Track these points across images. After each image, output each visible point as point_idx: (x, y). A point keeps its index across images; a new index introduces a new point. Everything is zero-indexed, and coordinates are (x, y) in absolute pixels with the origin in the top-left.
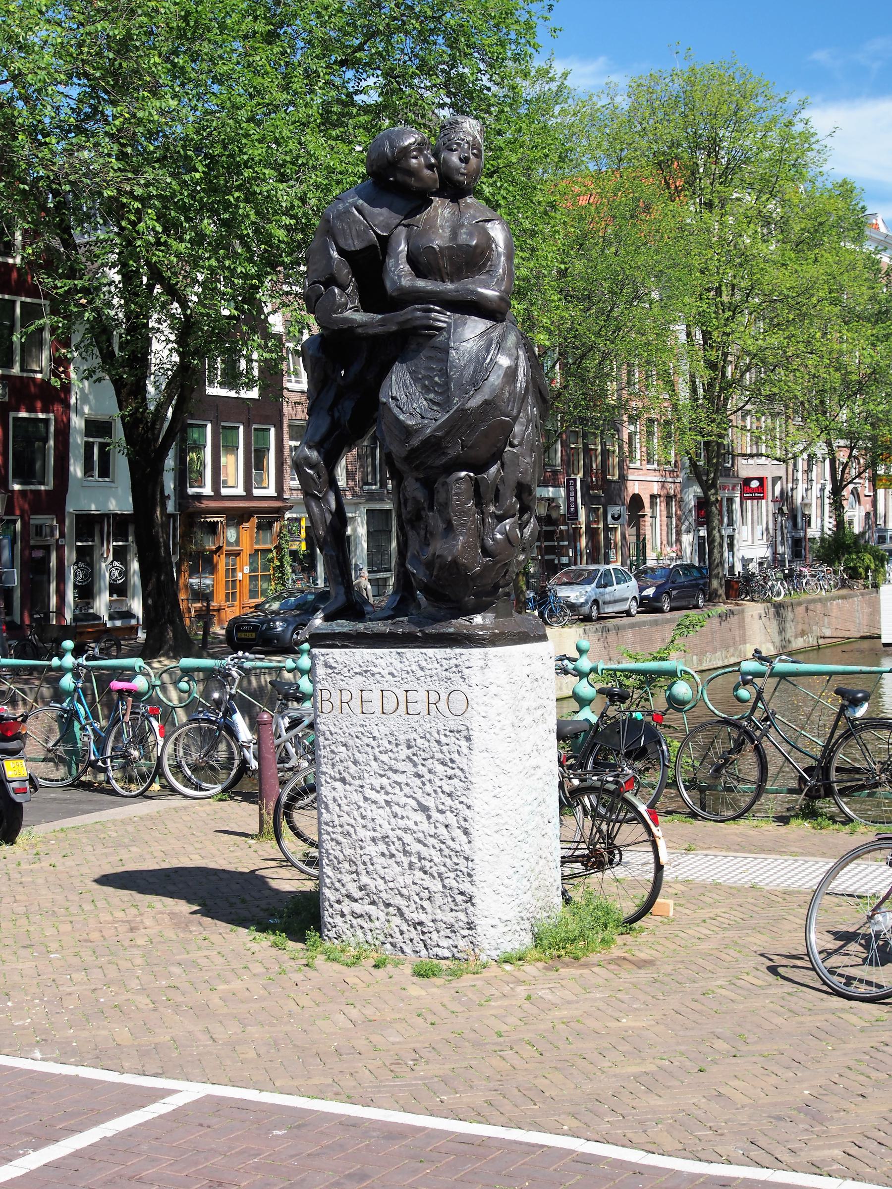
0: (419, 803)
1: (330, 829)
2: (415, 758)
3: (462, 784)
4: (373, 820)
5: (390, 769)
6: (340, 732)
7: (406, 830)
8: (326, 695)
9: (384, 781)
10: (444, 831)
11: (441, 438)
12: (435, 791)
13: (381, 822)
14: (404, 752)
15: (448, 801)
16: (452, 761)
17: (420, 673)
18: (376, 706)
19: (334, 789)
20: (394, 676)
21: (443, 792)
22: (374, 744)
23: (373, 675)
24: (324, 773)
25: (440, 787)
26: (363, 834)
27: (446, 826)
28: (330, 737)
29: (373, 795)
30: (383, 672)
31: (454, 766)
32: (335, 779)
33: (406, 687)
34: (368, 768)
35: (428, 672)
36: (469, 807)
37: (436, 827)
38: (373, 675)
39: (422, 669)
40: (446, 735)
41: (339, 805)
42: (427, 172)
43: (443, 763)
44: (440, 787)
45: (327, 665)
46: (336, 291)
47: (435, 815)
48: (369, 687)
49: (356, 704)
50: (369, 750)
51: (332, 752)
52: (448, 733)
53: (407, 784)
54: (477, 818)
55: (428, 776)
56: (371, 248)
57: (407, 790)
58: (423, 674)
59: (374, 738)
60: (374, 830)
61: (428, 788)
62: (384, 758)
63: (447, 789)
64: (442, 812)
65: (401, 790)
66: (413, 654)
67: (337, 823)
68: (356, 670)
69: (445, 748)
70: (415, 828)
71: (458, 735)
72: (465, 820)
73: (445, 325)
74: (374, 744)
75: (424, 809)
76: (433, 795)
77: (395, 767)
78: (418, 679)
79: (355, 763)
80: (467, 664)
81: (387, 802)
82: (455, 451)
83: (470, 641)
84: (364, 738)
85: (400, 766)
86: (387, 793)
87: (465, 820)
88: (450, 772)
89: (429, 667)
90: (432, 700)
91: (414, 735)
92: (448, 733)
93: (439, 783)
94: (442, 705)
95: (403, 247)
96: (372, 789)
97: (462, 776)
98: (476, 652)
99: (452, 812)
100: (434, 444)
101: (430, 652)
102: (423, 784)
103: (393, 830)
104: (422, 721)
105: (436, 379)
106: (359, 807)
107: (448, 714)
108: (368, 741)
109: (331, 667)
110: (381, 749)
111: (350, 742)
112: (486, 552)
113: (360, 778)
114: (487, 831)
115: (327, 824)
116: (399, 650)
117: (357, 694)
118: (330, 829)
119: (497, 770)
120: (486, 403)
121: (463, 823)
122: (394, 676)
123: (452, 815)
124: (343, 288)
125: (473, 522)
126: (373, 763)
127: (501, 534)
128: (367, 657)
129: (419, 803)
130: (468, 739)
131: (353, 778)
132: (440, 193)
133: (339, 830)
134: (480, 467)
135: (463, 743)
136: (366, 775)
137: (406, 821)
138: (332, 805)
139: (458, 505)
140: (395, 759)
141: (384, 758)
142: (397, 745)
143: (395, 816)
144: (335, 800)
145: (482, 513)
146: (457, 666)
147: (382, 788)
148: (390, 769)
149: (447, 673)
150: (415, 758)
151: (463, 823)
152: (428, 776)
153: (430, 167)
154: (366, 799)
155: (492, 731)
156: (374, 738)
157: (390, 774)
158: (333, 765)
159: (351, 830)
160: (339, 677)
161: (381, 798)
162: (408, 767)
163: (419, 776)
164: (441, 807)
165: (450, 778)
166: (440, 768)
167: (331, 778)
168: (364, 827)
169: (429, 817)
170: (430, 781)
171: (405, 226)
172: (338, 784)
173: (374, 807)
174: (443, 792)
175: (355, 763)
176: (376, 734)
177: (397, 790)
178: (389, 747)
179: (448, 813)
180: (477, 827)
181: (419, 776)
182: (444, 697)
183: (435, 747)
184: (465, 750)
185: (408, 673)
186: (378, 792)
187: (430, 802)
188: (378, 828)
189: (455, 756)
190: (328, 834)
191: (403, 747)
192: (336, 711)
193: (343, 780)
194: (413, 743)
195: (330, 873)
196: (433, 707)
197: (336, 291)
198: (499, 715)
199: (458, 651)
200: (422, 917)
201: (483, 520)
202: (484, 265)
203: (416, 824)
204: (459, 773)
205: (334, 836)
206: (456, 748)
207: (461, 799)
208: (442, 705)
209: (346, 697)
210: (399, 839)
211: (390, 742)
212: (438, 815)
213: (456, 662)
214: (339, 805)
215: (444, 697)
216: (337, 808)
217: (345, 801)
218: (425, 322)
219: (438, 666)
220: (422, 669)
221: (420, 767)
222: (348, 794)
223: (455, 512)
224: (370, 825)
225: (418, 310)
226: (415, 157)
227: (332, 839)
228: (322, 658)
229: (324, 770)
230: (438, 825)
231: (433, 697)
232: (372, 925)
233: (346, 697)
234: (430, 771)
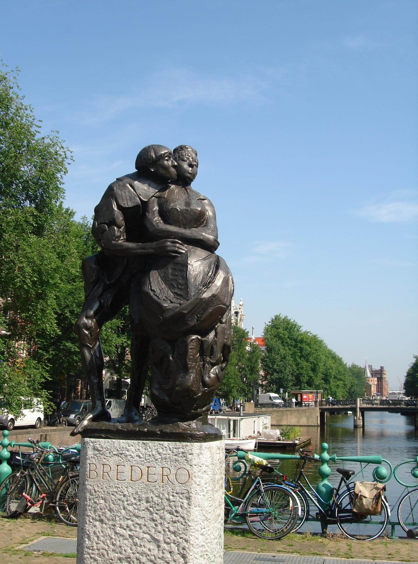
0: (151, 536)
2: (151, 509)
3: (183, 526)
4: (120, 547)
5: (134, 515)
6: (101, 490)
7: (142, 554)
9: (130, 522)
10: (169, 556)
11: (186, 314)
12: (164, 530)
13: (126, 548)
14: (144, 505)
15: (173, 537)
16: (177, 512)
17: (158, 456)
19: (95, 526)
20: (140, 457)
21: (169, 531)
22: (123, 498)
23: (126, 456)
24: (88, 516)
25: (168, 528)
26: (113, 555)
27: (170, 552)
28: (94, 494)
29: (122, 531)
30: (133, 455)
31: (178, 515)
32: (96, 520)
33: (148, 464)
34: (119, 514)
35: (164, 456)
36: (186, 541)
37: (163, 553)
38: (126, 456)
39: (159, 454)
40: (173, 496)
41: (98, 537)
42: (173, 170)
43: (171, 513)
44: (168, 528)
45: (95, 449)
46: (116, 228)
47: (163, 545)
49: (113, 474)
50: (120, 503)
51: (95, 503)
52: (175, 495)
53: (145, 525)
54: (191, 548)
55: (159, 521)
56: (137, 207)
57: (144, 528)
58: (160, 457)
59: (124, 496)
60: (121, 553)
61: (159, 528)
62: (131, 508)
63: (172, 529)
64: (168, 543)
65: (141, 528)
66: (153, 446)
67: (95, 547)
68: (114, 453)
69: (172, 504)
70: (149, 552)
71: (181, 496)
72: (184, 549)
73: (184, 252)
74: (123, 498)
75: (156, 541)
76: (163, 532)
77: (137, 514)
78: (156, 460)
79: (111, 510)
80: (190, 451)
81: (130, 536)
82: (193, 323)
83: (192, 438)
85: (141, 514)
86: (131, 530)
87: (184, 549)
88: (175, 519)
89: (165, 452)
90: (165, 473)
91: (152, 495)
92: (175, 495)
93: (167, 525)
95: (156, 208)
96: (121, 527)
97: (183, 521)
98: (196, 445)
99: (175, 543)
101: (166, 443)
102: (156, 525)
104: (157, 486)
105: (180, 281)
106: (111, 538)
107: (176, 482)
108: (120, 497)
109: (98, 450)
110: (129, 502)
111: (108, 498)
112: (205, 384)
113: (113, 520)
114: (196, 556)
115: (88, 548)
116: (145, 442)
117: (114, 467)
119: (203, 518)
120: (213, 296)
121: (182, 551)
122: (140, 457)
123: (174, 545)
124: (119, 227)
125: (199, 365)
126: (123, 511)
127: (214, 374)
128: (122, 445)
129: (151, 536)
130: (188, 498)
131: (108, 520)
132: (175, 182)
133: (97, 552)
134: (205, 333)
135: (185, 501)
136: (117, 518)
137: (143, 548)
138: (92, 536)
139: (191, 355)
140: (138, 509)
141: (131, 508)
142: (139, 500)
143: (136, 544)
144: (95, 533)
145: (204, 361)
146: (183, 453)
147: (128, 527)
148: (134, 515)
149: (176, 457)
150: (151, 509)
151: (182, 551)
152: (159, 521)
153: (174, 166)
154: (116, 533)
155: (202, 494)
156: (124, 496)
157: (134, 518)
158: (95, 511)
159: (105, 553)
160: (102, 456)
161: (127, 533)
162: (147, 515)
163: (154, 520)
164: (168, 540)
165: (175, 522)
166: (168, 516)
167: (93, 519)
168: (113, 551)
169: (159, 546)
170: (161, 524)
171: (156, 197)
172: (97, 523)
173: (121, 538)
174: (169, 531)
175: (111, 510)
176: (126, 493)
177: (138, 529)
178: (134, 501)
179: (172, 545)
180: (191, 553)
181: (154, 520)
183: (166, 503)
184: (186, 505)
185: (150, 456)
186: (125, 529)
187: (160, 537)
188: (124, 552)
189: (179, 509)
190: (89, 554)
191: (144, 502)
193: (102, 521)
194: (151, 500)
197: (116, 228)
198: (206, 484)
199: (184, 444)
201: (204, 365)
202: (203, 222)
203: (150, 550)
204: (182, 520)
205: (93, 556)
206: (180, 504)
207: (182, 536)
209: (107, 469)
210: (137, 559)
211: (135, 498)
212: (165, 545)
213: (182, 450)
214: (98, 537)
215: (173, 471)
216: (96, 539)
217: (102, 534)
218: (173, 248)
219: (170, 452)
220: (159, 454)
221: (155, 515)
222: (105, 530)
223: (190, 359)
224: (118, 550)
225: (169, 241)
226: (167, 160)
227: (91, 558)
228: (92, 444)
229: (89, 514)
230: (165, 551)
231: (166, 472)
233: (107, 469)
234: (161, 518)
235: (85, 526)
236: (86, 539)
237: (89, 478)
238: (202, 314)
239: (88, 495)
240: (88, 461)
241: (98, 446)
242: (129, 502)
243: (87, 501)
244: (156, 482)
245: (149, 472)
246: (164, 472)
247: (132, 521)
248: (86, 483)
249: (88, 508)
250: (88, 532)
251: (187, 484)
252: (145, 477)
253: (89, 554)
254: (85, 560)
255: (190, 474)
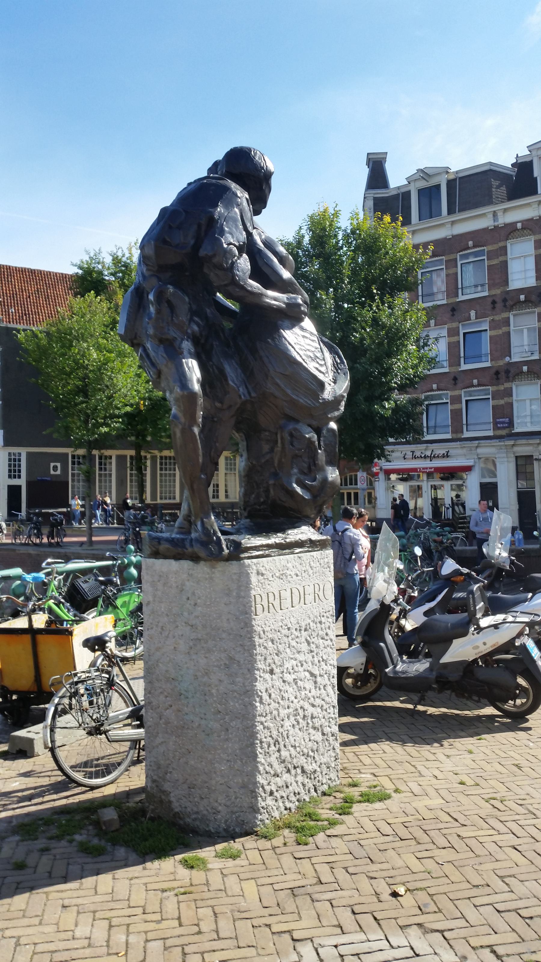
1: (263, 719)
8: (258, 599)
17: (311, 572)
24: (258, 670)
33: (304, 583)
65: (302, 665)
84: (283, 631)
88: (326, 643)
109: (263, 575)
118: (263, 719)
138: (265, 696)
176: (289, 625)
190: (262, 723)
195: (263, 761)
228: (254, 567)
229: (260, 666)
235: (255, 686)
236: (258, 704)
237: (256, 615)
239: (257, 639)
240: (253, 593)
241: (262, 569)
242: (293, 636)
243: (256, 650)
247: (296, 660)
248: (253, 623)
249: (259, 657)
250: (260, 693)
253: (262, 723)
254: (258, 735)
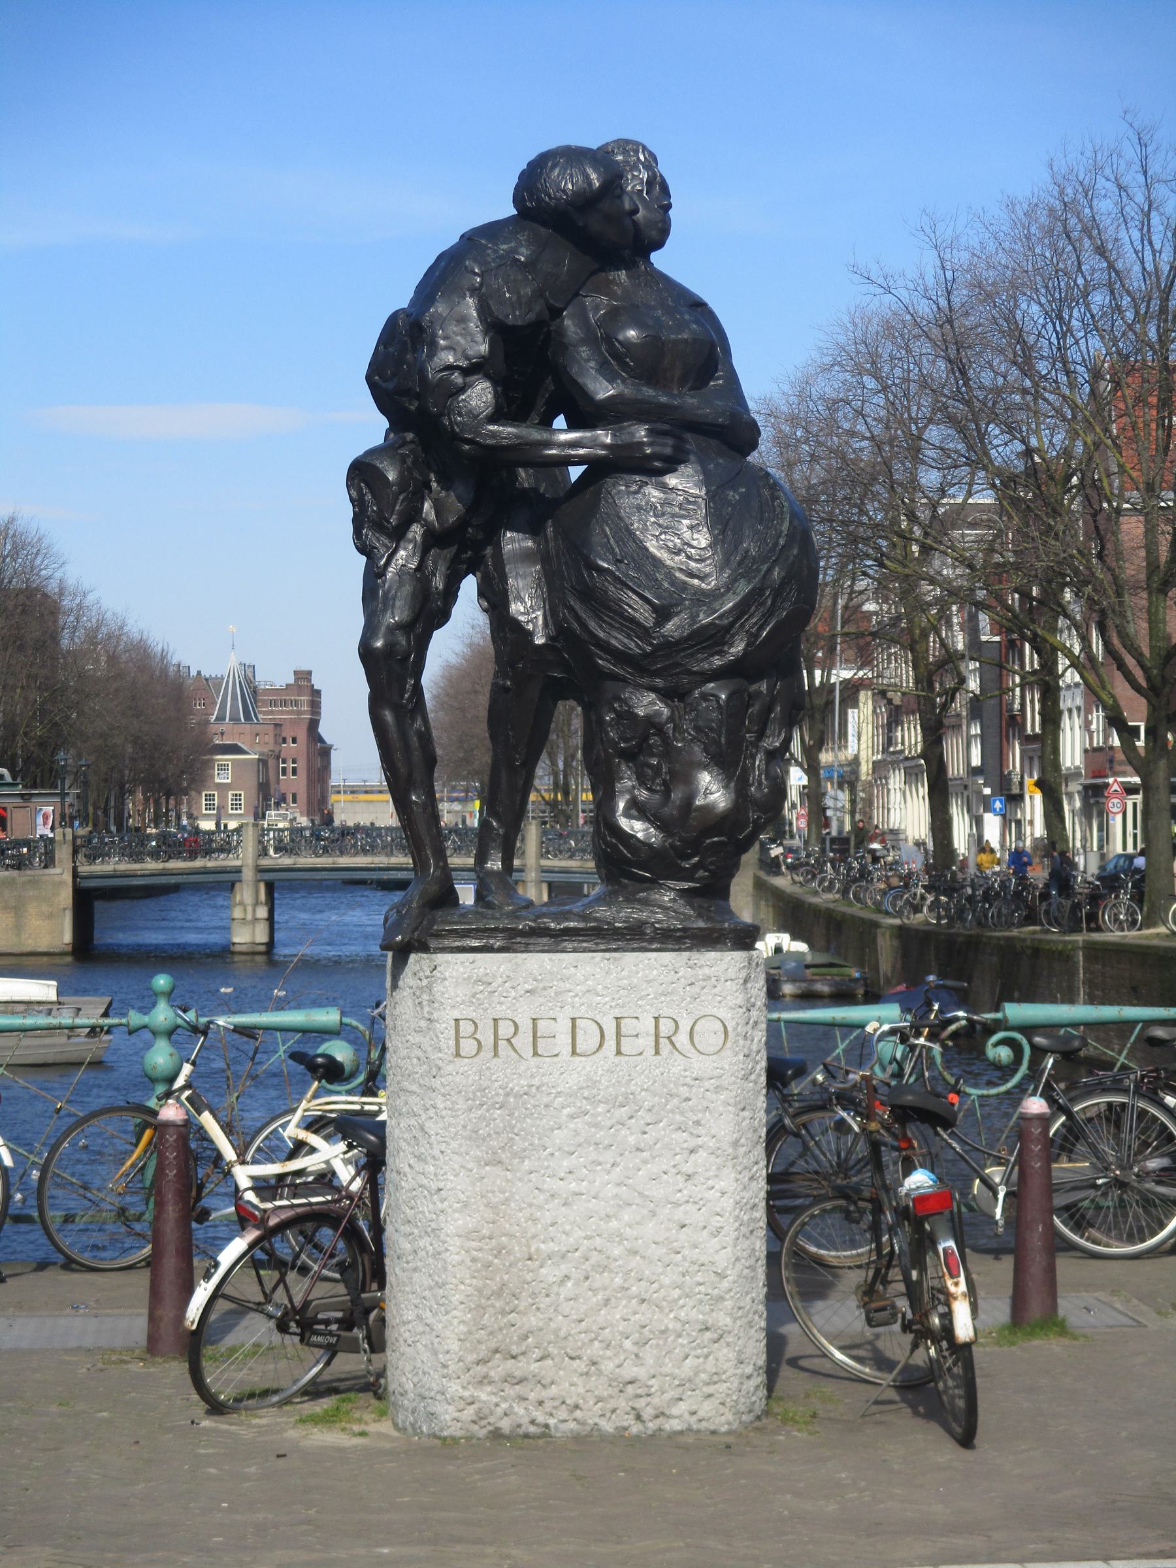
18: (564, 1040)
48: (551, 1014)
49: (523, 1041)
82: (738, 648)
94: (682, 1039)
100: (712, 638)
101: (667, 957)
103: (587, 1238)
140: (596, 1125)
141: (579, 1123)
182: (685, 1027)
192: (487, 1053)
196: (663, 1042)
200: (640, 1372)
208: (682, 1039)
215: (685, 1027)
231: (666, 1027)
232: (545, 1394)
238: (761, 628)
244: (641, 1054)
245: (623, 1030)
246: (662, 1028)
251: (723, 1053)
252: (610, 1043)
255: (730, 1029)
